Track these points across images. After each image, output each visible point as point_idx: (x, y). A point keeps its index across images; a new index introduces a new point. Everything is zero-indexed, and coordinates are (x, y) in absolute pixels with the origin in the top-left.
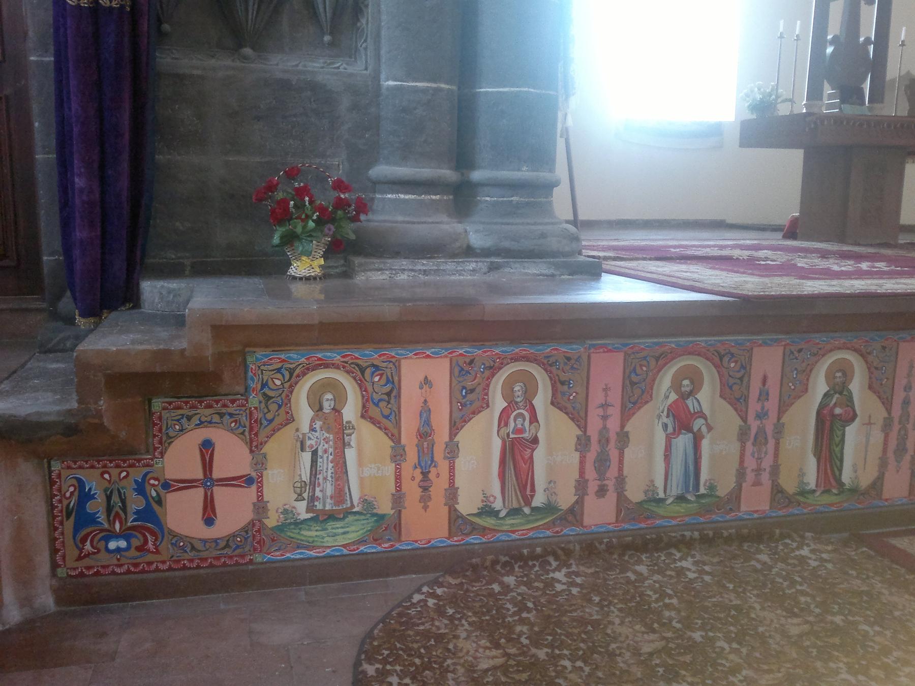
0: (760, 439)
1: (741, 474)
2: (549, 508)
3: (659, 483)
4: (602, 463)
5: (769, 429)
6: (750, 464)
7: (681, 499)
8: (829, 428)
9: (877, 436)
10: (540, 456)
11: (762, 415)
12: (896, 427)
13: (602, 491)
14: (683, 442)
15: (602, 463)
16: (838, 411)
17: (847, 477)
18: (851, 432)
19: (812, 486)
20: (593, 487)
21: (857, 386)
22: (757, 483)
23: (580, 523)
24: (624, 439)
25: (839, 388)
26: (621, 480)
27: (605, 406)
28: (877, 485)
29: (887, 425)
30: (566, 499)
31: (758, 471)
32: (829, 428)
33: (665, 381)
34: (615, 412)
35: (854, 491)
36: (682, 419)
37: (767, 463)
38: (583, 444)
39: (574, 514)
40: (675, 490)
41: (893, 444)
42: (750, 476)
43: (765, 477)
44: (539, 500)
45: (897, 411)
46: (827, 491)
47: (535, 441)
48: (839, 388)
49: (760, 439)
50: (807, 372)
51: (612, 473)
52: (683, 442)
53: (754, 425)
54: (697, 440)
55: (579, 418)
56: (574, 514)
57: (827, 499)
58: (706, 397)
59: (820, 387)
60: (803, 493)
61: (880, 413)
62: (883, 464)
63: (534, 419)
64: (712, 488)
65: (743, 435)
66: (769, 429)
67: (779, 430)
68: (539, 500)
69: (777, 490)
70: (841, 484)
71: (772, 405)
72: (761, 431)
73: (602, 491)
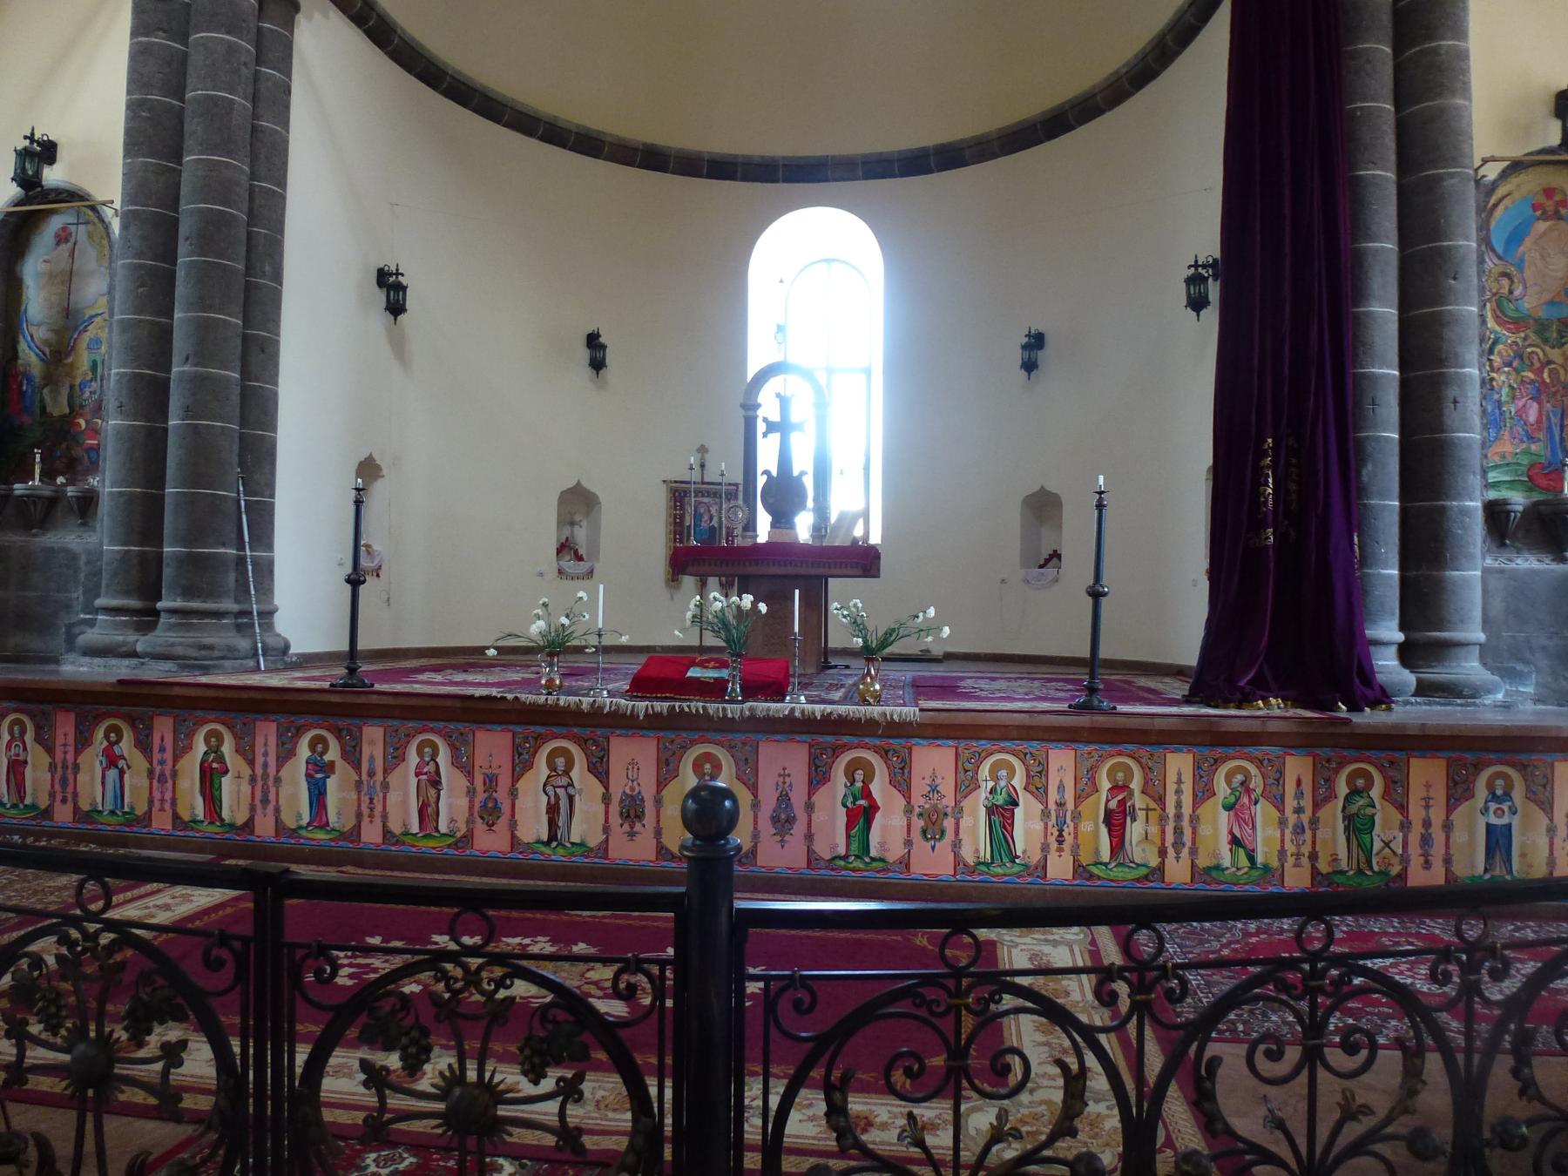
0: (162, 779)
1: (151, 802)
2: (34, 807)
3: (99, 800)
4: (64, 781)
5: (168, 773)
6: (157, 795)
7: (112, 812)
8: (210, 777)
9: (246, 788)
10: (28, 772)
11: (162, 762)
12: (260, 783)
13: (64, 801)
14: (112, 774)
15: (64, 781)
16: (215, 765)
17: (225, 814)
18: (226, 782)
19: (201, 817)
20: (59, 797)
21: (227, 748)
22: (162, 809)
23: (51, 819)
24: (76, 767)
25: (214, 750)
26: (75, 794)
27: (65, 745)
28: (249, 825)
29: (253, 779)
30: (43, 803)
31: (163, 800)
32: (210, 777)
33: (100, 734)
34: (71, 749)
35: (232, 826)
36: (112, 760)
37: (168, 796)
38: (52, 767)
39: (47, 813)
40: (109, 806)
41: (258, 795)
42: (157, 804)
43: (167, 806)
44: (28, 801)
45: (259, 771)
46: (211, 823)
47: (26, 762)
48: (214, 750)
49: (162, 779)
50: (190, 735)
51: (70, 789)
52: (112, 774)
53: (158, 769)
54: (122, 773)
55: (50, 750)
56: (47, 813)
57: (212, 828)
58: (126, 746)
59: (200, 747)
60: (195, 821)
61: (246, 771)
62: (253, 809)
63: (25, 749)
64: (132, 808)
65: (151, 773)
66: (168, 773)
67: (174, 774)
68: (28, 801)
69: (176, 817)
70: (222, 820)
71: (169, 755)
72: (162, 774)
73: (64, 801)
